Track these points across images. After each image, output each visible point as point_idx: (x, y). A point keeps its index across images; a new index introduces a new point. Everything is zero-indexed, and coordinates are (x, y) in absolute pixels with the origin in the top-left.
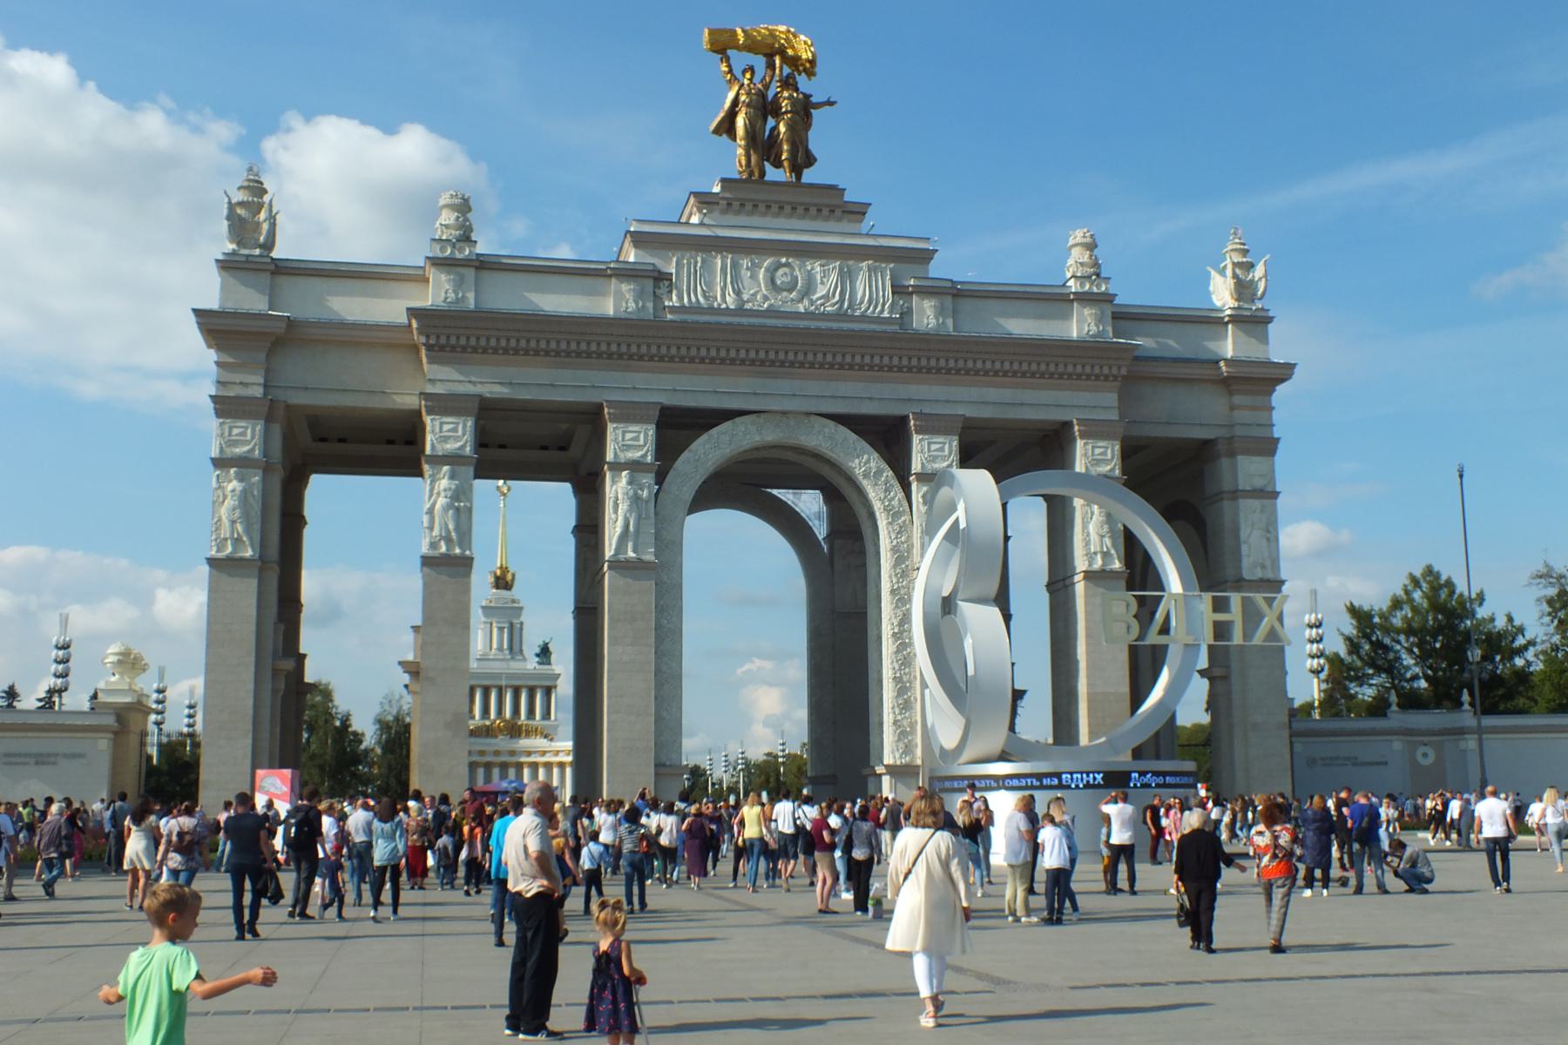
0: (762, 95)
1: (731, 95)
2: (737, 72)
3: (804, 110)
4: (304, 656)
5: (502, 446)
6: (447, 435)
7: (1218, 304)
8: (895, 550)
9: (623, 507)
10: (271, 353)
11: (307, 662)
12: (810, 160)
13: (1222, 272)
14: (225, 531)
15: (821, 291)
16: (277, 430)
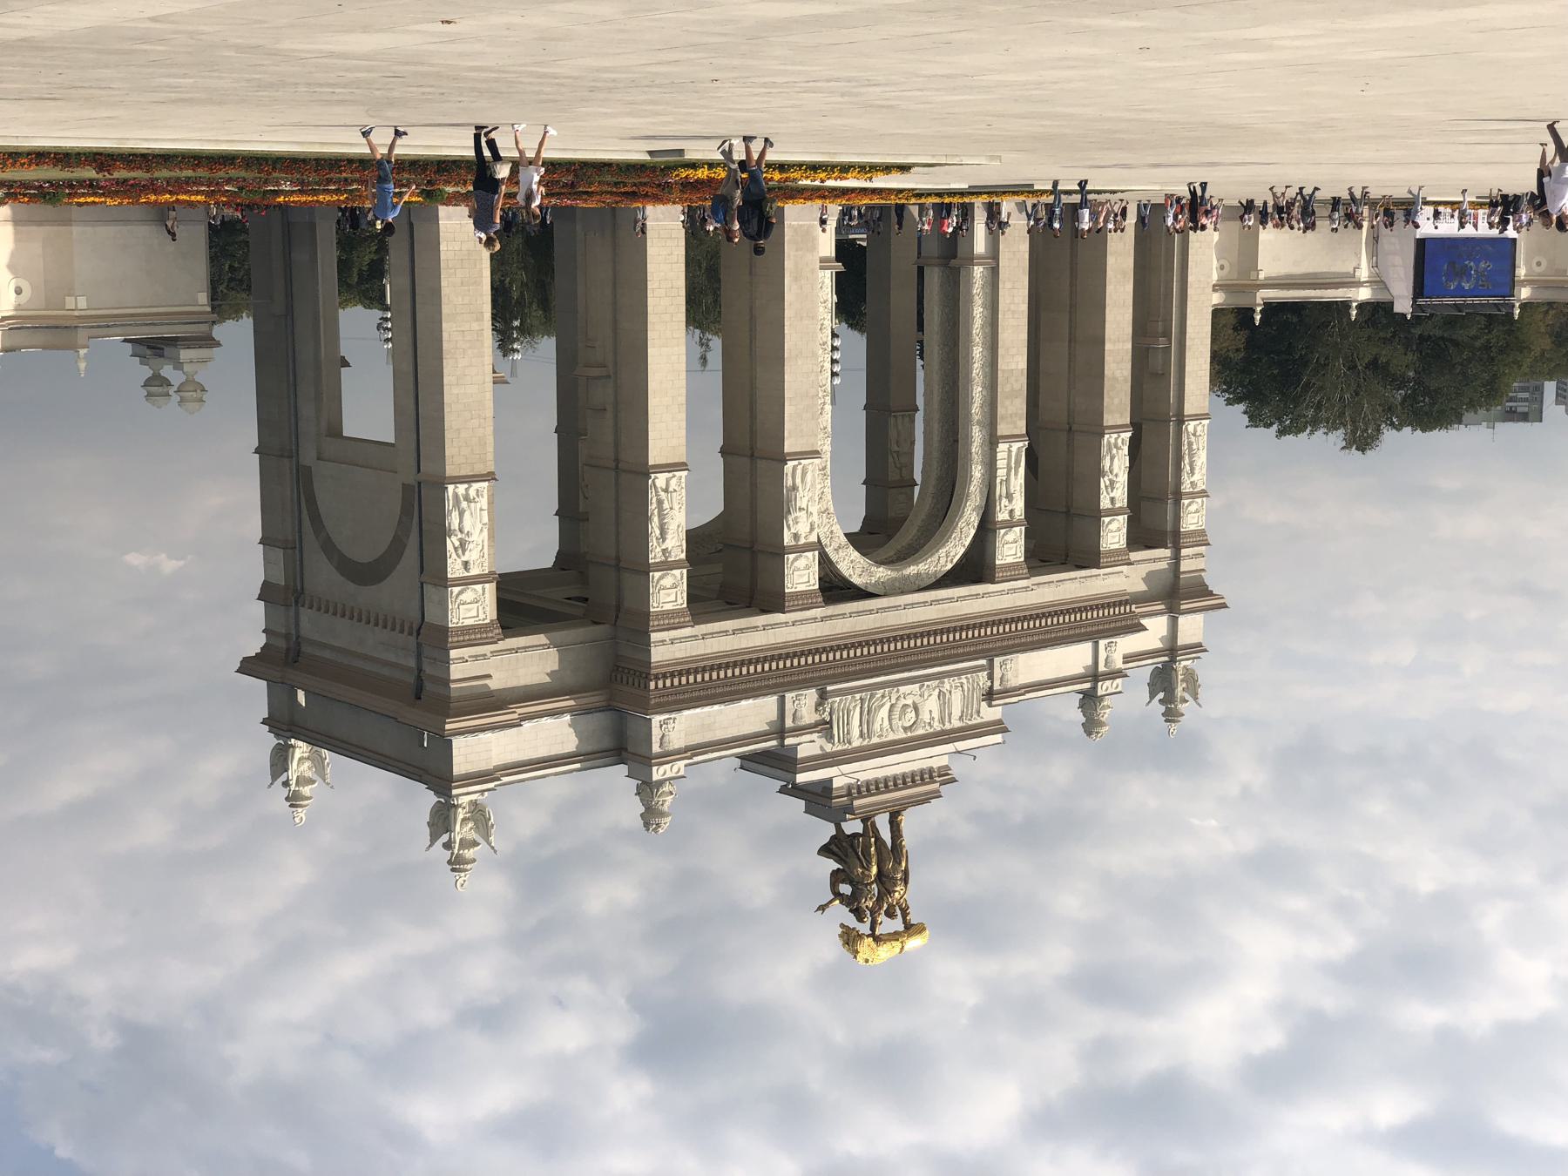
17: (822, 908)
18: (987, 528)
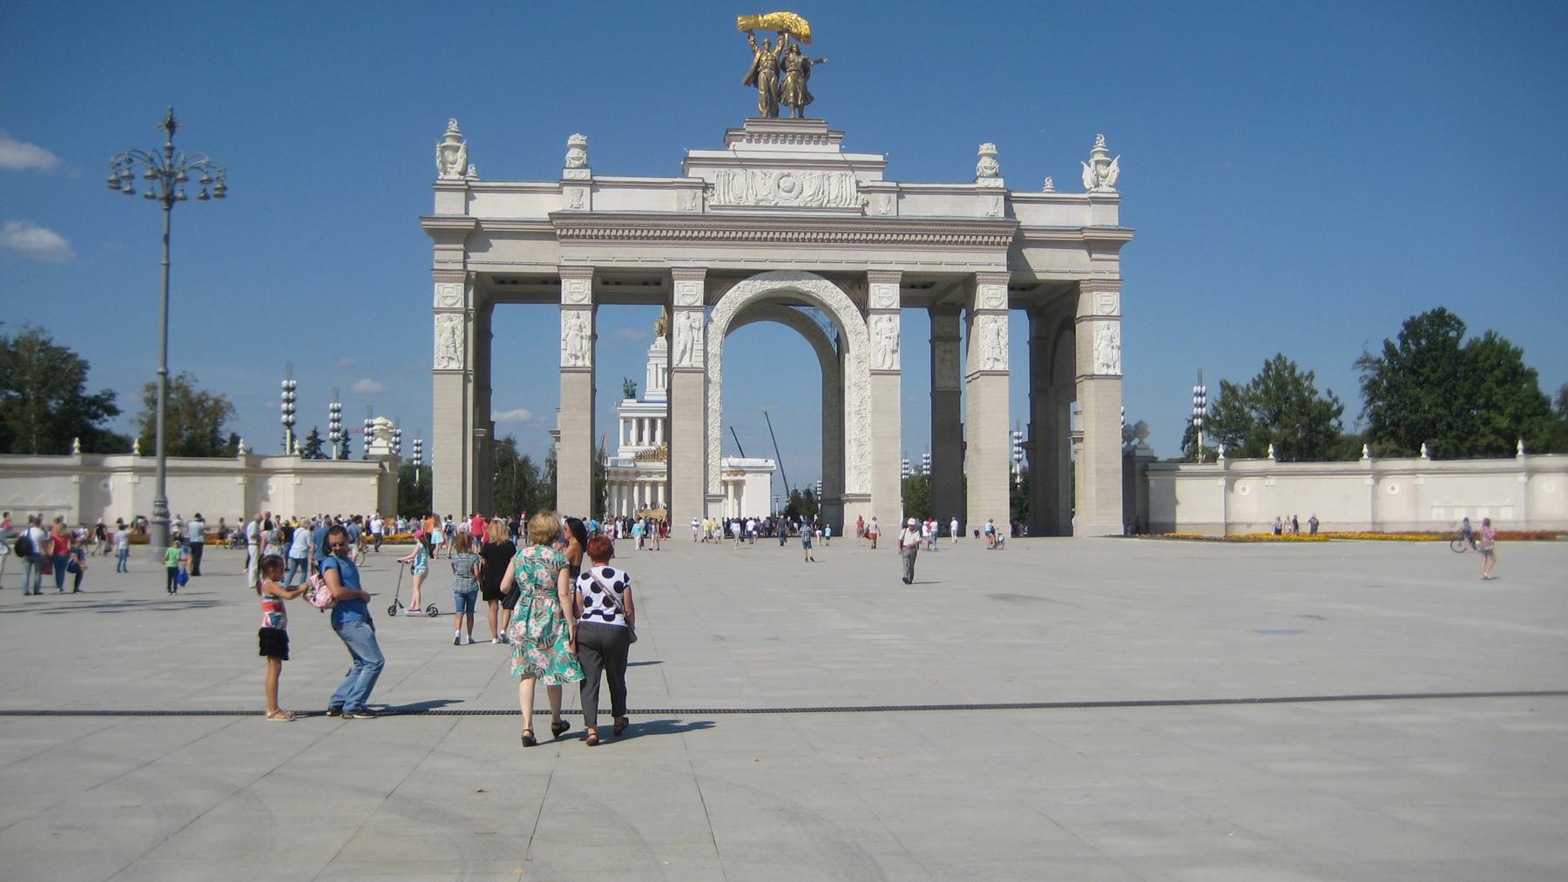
3: (805, 69)
5: (618, 283)
6: (576, 290)
15: (808, 192)
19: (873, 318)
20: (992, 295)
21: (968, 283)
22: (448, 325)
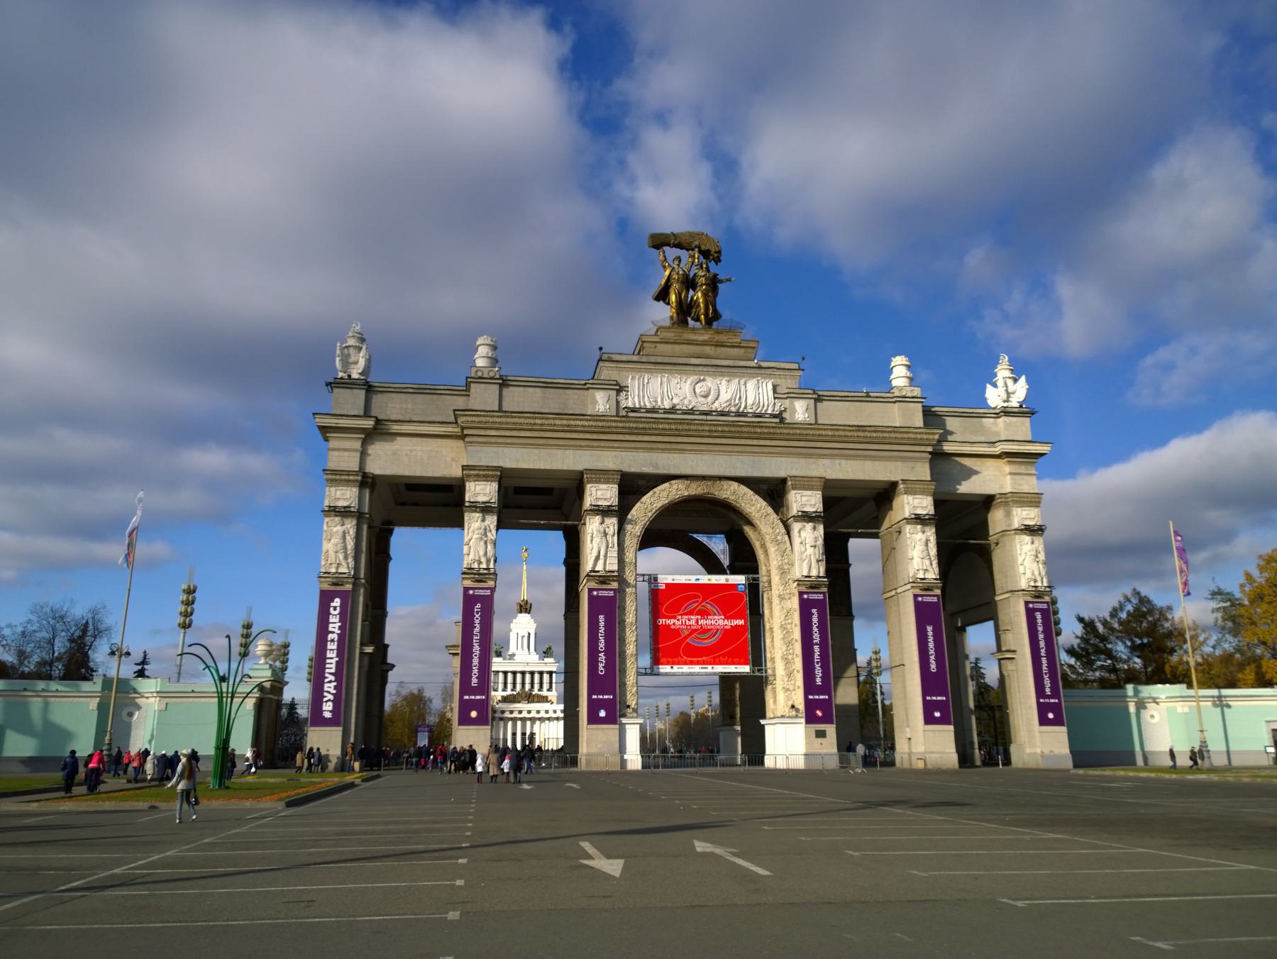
0: (686, 275)
1: (667, 273)
2: (670, 259)
4: (387, 646)
7: (993, 405)
8: (780, 568)
9: (596, 540)
10: (365, 442)
11: (390, 650)
12: (717, 316)
13: (995, 385)
14: (332, 558)
16: (367, 493)
17: (729, 280)
18: (621, 512)
19: (796, 527)
20: (918, 503)
21: (884, 495)
22: (339, 529)
